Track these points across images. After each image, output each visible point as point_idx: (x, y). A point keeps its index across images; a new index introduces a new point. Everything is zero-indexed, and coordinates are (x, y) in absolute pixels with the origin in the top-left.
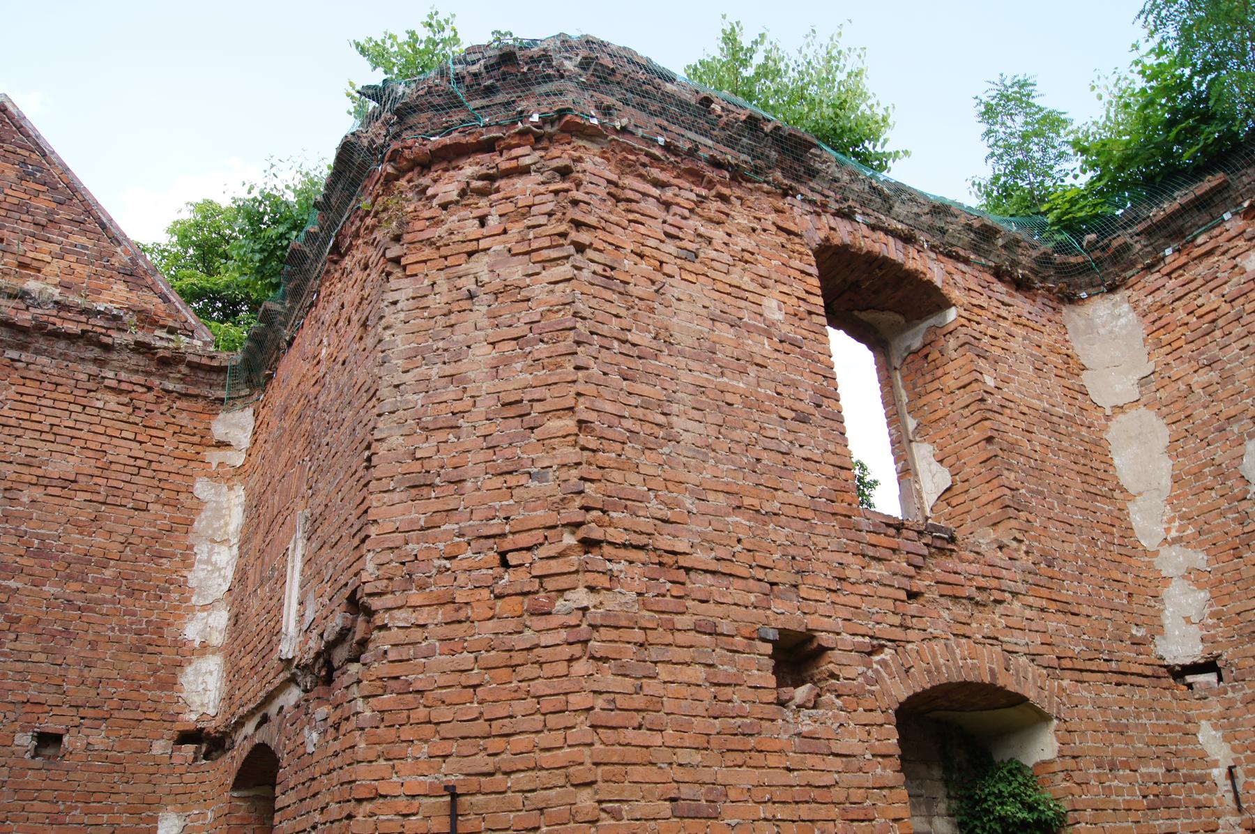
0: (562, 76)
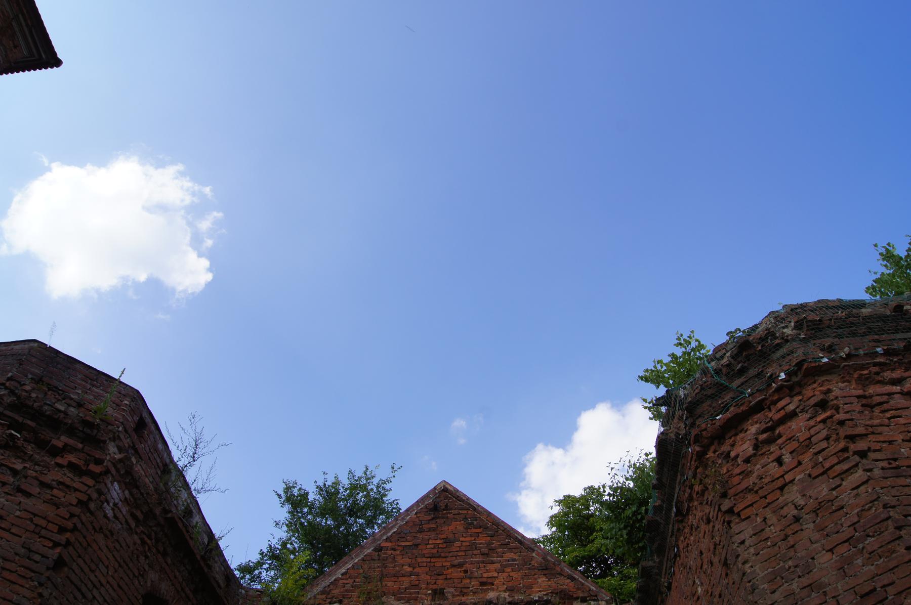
0: (787, 341)
